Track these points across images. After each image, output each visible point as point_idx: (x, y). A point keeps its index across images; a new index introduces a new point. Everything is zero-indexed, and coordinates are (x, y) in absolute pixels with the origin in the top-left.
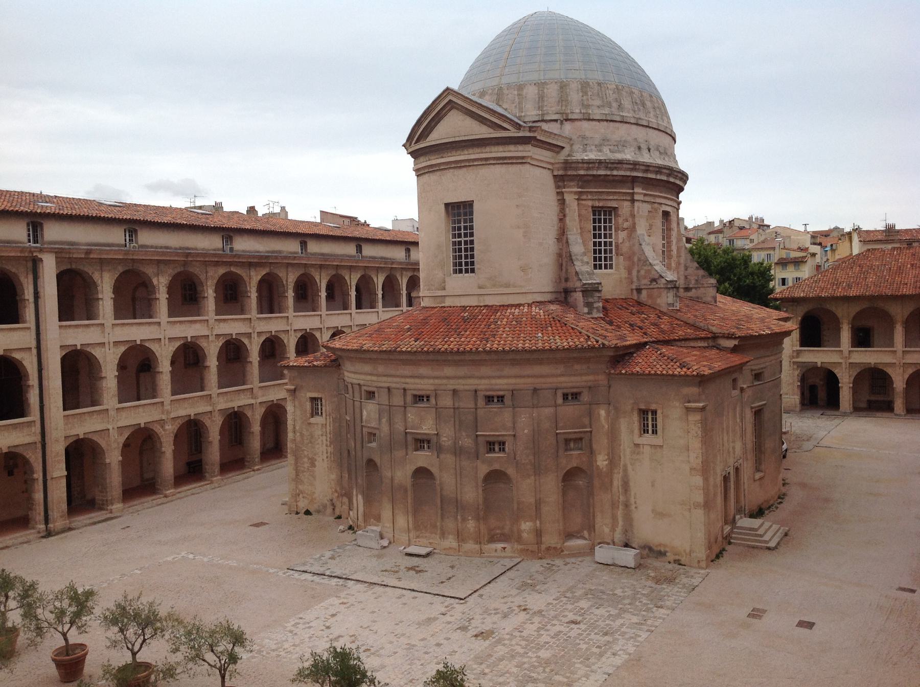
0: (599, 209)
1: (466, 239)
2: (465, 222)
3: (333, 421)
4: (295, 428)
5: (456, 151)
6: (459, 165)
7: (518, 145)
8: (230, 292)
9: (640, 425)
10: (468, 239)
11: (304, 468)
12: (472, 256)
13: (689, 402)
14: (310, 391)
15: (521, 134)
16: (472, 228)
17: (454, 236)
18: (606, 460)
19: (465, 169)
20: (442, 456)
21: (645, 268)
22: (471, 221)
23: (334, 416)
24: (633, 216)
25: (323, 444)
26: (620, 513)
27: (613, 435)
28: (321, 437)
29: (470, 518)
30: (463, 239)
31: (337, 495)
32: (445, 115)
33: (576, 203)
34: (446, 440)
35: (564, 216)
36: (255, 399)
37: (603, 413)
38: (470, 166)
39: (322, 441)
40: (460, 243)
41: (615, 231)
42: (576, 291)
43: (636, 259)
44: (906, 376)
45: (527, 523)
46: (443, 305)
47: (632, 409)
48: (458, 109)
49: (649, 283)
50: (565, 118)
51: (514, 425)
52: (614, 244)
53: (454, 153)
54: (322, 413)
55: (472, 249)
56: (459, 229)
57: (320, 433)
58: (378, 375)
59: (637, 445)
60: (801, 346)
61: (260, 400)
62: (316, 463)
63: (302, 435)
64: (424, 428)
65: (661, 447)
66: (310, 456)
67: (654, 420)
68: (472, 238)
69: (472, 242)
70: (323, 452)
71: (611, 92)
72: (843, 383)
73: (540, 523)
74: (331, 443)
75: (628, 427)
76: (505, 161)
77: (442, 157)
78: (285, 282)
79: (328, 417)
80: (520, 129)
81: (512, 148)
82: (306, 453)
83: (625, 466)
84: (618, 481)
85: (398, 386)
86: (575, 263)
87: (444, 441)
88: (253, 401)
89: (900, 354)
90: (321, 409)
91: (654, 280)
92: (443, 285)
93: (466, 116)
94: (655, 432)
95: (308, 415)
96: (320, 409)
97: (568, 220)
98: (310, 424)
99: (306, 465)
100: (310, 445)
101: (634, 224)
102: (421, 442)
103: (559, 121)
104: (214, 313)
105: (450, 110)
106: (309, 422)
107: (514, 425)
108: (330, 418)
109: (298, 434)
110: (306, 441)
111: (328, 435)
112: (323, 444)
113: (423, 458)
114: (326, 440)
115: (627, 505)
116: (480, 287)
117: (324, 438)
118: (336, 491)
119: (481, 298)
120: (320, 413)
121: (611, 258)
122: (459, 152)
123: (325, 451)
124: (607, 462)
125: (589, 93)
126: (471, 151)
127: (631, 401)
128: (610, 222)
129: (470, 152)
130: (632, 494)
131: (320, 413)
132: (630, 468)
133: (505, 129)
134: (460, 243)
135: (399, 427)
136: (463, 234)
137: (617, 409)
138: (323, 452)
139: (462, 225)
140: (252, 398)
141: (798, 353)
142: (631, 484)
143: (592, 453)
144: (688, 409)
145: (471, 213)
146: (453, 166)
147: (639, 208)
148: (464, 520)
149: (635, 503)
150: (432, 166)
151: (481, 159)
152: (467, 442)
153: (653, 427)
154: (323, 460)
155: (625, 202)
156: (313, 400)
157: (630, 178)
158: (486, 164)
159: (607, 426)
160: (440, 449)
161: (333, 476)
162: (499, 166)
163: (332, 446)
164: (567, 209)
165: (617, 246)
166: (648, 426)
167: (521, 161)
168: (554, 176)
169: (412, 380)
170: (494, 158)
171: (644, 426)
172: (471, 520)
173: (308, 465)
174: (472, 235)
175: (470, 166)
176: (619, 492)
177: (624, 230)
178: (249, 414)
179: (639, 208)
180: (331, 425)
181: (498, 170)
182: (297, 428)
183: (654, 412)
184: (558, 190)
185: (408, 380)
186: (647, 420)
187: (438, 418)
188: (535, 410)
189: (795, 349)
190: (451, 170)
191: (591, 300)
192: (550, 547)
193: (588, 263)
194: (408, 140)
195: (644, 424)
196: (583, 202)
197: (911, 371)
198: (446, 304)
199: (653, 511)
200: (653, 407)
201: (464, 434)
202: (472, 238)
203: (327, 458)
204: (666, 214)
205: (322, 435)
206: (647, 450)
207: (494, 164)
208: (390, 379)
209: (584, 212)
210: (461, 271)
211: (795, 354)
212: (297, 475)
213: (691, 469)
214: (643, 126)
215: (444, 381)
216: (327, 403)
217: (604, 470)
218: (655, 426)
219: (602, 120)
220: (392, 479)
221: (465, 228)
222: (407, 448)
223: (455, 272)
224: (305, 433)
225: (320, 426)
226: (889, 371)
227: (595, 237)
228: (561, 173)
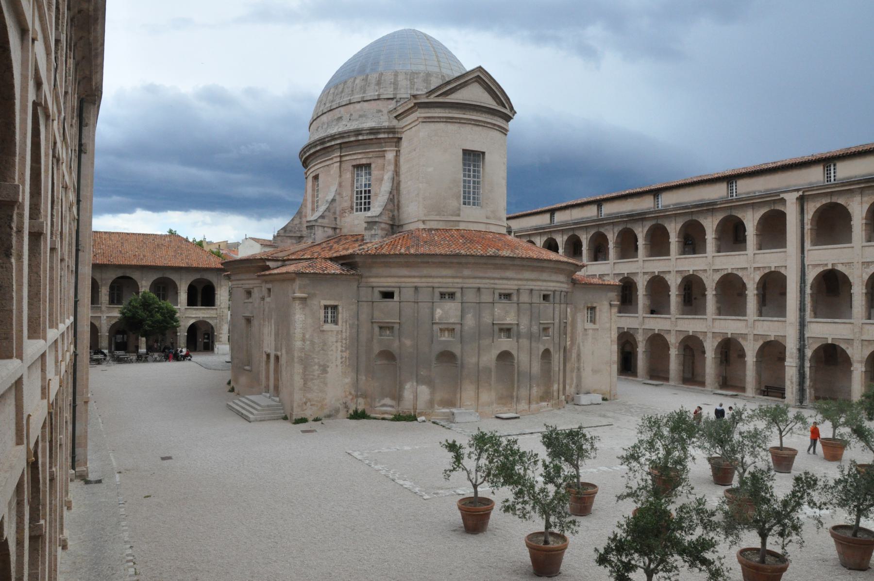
1: (474, 179)
2: (474, 166)
3: (350, 327)
4: (304, 336)
5: (477, 113)
6: (477, 123)
11: (314, 375)
14: (325, 299)
17: (464, 176)
19: (481, 128)
23: (351, 322)
25: (337, 350)
26: (574, 375)
31: (350, 397)
32: (468, 85)
38: (484, 126)
39: (337, 347)
40: (469, 182)
41: (460, 195)
46: (457, 228)
47: (584, 306)
48: (480, 84)
53: (475, 113)
57: (334, 339)
58: (463, 278)
59: (586, 330)
62: (329, 369)
63: (313, 343)
64: (508, 319)
66: (322, 363)
70: (336, 358)
74: (346, 349)
75: (582, 318)
77: (464, 114)
79: (344, 324)
85: (486, 286)
87: (522, 329)
92: (458, 212)
93: (484, 91)
95: (322, 323)
98: (323, 331)
99: (316, 373)
100: (322, 352)
102: (507, 331)
106: (321, 329)
108: (346, 325)
109: (308, 342)
110: (317, 349)
113: (505, 344)
114: (342, 346)
115: (579, 369)
116: (487, 218)
117: (339, 344)
118: (350, 394)
119: (488, 226)
122: (479, 114)
123: (339, 358)
126: (487, 116)
130: (582, 361)
132: (581, 344)
133: (505, 107)
135: (487, 319)
136: (472, 175)
137: (576, 307)
138: (336, 358)
139: (472, 168)
142: (582, 355)
144: (611, 305)
146: (473, 123)
154: (337, 366)
156: (326, 307)
160: (519, 336)
161: (348, 380)
162: (498, 132)
163: (348, 352)
169: (501, 282)
173: (319, 372)
175: (484, 126)
180: (348, 331)
182: (307, 336)
183: (594, 308)
185: (497, 281)
190: (470, 126)
194: (427, 93)
198: (461, 228)
199: (592, 370)
200: (594, 305)
203: (342, 363)
205: (337, 342)
206: (590, 332)
208: (478, 281)
212: (305, 384)
215: (524, 283)
216: (344, 310)
221: (474, 171)
223: (464, 204)
224: (316, 341)
225: (335, 333)
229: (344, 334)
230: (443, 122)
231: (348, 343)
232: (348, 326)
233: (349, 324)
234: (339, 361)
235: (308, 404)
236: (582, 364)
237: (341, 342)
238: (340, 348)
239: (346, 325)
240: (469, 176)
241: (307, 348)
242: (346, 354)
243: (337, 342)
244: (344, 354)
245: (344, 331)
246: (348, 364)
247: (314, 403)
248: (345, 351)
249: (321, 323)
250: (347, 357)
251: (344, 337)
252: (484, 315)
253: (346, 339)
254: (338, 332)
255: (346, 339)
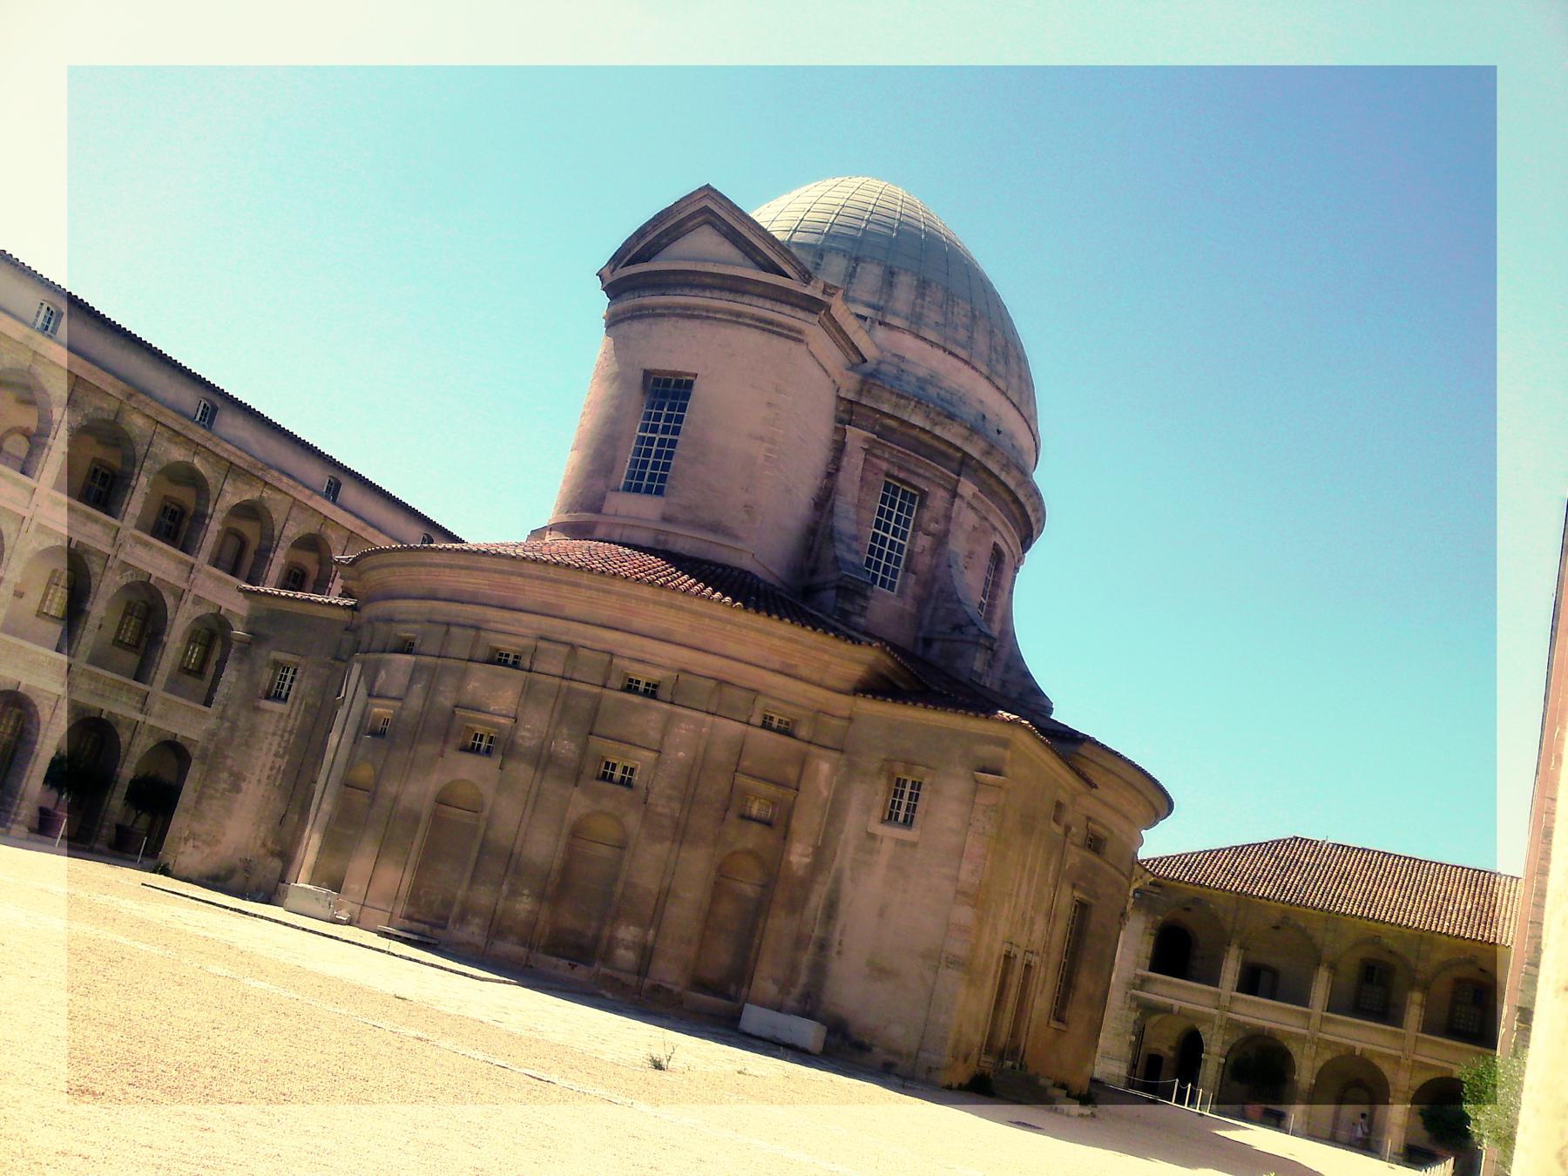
0: (898, 484)
1: (663, 436)
3: (305, 710)
6: (688, 314)
7: (797, 309)
8: (168, 522)
9: (887, 800)
10: (669, 437)
11: (217, 790)
12: (666, 467)
13: (983, 770)
15: (808, 291)
16: (680, 419)
17: (644, 428)
18: (807, 856)
19: (697, 322)
20: (511, 765)
21: (949, 605)
22: (683, 408)
23: (310, 701)
24: (948, 518)
25: (269, 750)
27: (835, 812)
28: (269, 737)
29: (526, 892)
30: (657, 436)
33: (862, 455)
34: (527, 736)
35: (838, 470)
36: (146, 714)
37: (825, 767)
38: (708, 317)
42: (825, 589)
43: (937, 587)
44: (1320, 1064)
45: (632, 928)
47: (881, 770)
49: (949, 631)
50: (880, 318)
51: (663, 738)
52: (905, 551)
54: (287, 695)
55: (670, 455)
56: (658, 417)
59: (872, 836)
60: (1152, 969)
61: (151, 721)
62: (244, 785)
65: (914, 845)
67: (914, 797)
68: (675, 437)
69: (673, 443)
71: (962, 313)
72: (1208, 1053)
73: (656, 935)
76: (770, 327)
78: (276, 533)
79: (298, 702)
80: (808, 283)
81: (787, 309)
82: (229, 762)
83: (840, 872)
84: (820, 897)
86: (836, 544)
87: (523, 737)
88: (140, 717)
89: (1315, 1021)
90: (290, 687)
91: (958, 628)
93: (724, 239)
94: (908, 822)
96: (286, 687)
97: (841, 475)
101: (946, 533)
103: (868, 319)
104: (134, 522)
105: (700, 225)
106: (256, 704)
107: (663, 738)
108: (301, 704)
111: (286, 738)
112: (269, 750)
114: (279, 745)
115: (823, 946)
117: (277, 739)
120: (283, 695)
121: (895, 572)
122: (695, 292)
123: (269, 765)
124: (807, 860)
125: (928, 299)
127: (883, 756)
128: (909, 513)
129: (715, 296)
130: (838, 927)
131: (283, 695)
132: (847, 875)
134: (651, 441)
135: (445, 700)
136: (660, 427)
137: (852, 765)
138: (264, 766)
140: (141, 711)
141: (1143, 983)
142: (842, 907)
143: (785, 838)
145: (687, 396)
147: (960, 508)
148: (514, 893)
149: (840, 944)
150: (641, 308)
151: (730, 312)
152: (566, 747)
153: (907, 809)
154: (259, 781)
155: (941, 490)
156: (277, 665)
157: (959, 455)
158: (736, 322)
159: (825, 793)
163: (287, 757)
164: (845, 459)
165: (910, 554)
166: (899, 808)
167: (795, 336)
168: (838, 397)
170: (753, 317)
171: (893, 807)
172: (528, 896)
173: (226, 786)
174: (676, 431)
175: (708, 317)
176: (815, 919)
177: (928, 533)
178: (125, 737)
179: (960, 508)
180: (299, 718)
181: (753, 339)
182: (230, 713)
183: (917, 786)
184: (839, 425)
185: (492, 614)
186: (901, 797)
187: (528, 692)
188: (709, 718)
189: (1140, 972)
191: (848, 607)
192: (659, 985)
193: (857, 553)
195: (894, 802)
196: (875, 460)
197: (1328, 1056)
201: (565, 731)
202: (675, 437)
203: (269, 777)
204: (997, 556)
205: (274, 734)
206: (887, 848)
207: (749, 325)
209: (870, 477)
210: (637, 489)
211: (1138, 982)
213: (957, 892)
214: (998, 389)
217: (801, 873)
218: (912, 809)
219: (938, 346)
220: (396, 799)
222: (445, 742)
226: (1293, 1048)
227: (878, 526)
228: (850, 396)
229: (291, 721)
230: (629, 318)
231: (292, 741)
232: (303, 708)
233: (306, 704)
234: (267, 772)
235: (191, 843)
236: (837, 936)
237: (282, 736)
238: (274, 748)
239: (301, 704)
240: (654, 429)
241: (223, 734)
242: (282, 763)
243: (274, 734)
244: (279, 761)
245: (293, 715)
246: (277, 784)
247: (200, 844)
248: (282, 757)
249: (260, 692)
250: (282, 768)
251: (289, 729)
252: (442, 689)
253: (291, 732)
254: (281, 715)
255: (291, 732)
